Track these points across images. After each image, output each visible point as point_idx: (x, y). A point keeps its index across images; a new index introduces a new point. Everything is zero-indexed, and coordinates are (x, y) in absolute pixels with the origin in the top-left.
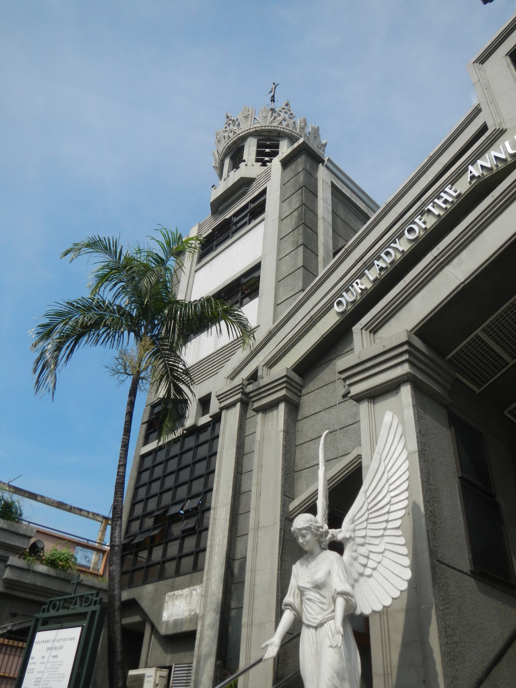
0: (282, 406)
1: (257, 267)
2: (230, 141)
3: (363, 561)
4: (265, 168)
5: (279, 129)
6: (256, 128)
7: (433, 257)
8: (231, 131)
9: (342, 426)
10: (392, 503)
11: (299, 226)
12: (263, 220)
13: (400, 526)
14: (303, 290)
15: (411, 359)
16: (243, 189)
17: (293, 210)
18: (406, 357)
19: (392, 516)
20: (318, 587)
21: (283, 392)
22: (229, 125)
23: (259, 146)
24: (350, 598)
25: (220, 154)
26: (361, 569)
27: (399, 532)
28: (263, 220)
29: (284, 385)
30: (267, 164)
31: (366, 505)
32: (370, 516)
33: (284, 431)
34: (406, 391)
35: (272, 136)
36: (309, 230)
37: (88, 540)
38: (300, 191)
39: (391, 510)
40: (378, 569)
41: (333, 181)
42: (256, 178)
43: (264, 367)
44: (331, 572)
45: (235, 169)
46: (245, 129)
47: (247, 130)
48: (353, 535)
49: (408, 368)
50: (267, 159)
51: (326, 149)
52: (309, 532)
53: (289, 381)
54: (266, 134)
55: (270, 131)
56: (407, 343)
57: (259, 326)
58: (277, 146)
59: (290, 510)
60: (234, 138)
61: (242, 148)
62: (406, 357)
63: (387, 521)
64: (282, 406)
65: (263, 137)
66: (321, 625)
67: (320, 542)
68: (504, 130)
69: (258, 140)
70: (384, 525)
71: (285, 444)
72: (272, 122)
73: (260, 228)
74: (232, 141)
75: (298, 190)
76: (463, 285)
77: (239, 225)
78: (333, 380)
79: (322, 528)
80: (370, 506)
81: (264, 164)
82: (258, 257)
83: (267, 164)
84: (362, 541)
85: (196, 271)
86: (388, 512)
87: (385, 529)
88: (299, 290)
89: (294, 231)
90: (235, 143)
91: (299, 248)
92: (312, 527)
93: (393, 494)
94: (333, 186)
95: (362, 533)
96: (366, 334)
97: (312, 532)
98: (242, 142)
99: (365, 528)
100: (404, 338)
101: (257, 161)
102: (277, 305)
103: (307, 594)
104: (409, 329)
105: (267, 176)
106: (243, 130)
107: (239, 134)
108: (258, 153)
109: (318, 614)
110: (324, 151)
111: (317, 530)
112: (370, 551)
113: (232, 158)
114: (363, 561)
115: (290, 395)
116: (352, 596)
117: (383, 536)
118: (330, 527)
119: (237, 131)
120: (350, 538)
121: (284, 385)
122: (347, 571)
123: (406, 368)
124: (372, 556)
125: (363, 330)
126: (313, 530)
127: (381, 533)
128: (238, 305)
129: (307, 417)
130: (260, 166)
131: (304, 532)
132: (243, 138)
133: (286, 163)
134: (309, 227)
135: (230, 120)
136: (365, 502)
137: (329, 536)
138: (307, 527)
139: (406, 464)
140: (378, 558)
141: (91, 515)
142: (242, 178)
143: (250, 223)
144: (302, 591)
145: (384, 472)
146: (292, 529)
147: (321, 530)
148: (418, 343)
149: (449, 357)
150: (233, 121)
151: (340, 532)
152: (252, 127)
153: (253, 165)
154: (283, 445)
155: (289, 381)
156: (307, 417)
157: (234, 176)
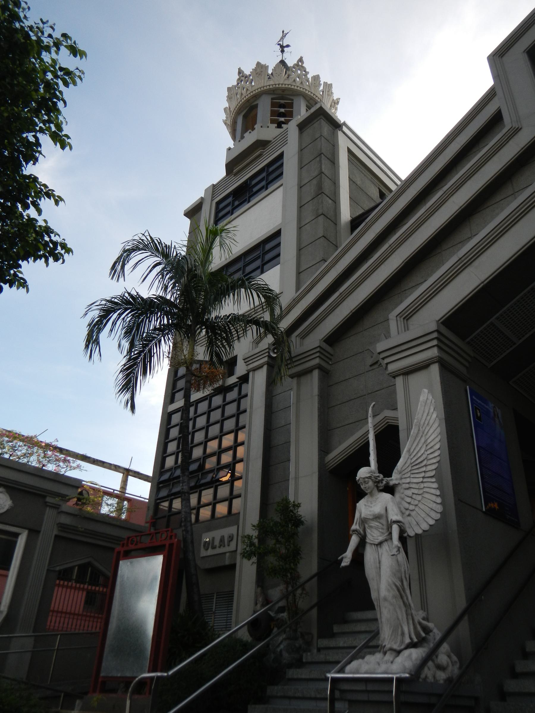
0: (316, 373)
1: (277, 234)
2: (243, 99)
3: (409, 500)
4: (280, 130)
5: (293, 87)
6: (269, 85)
7: (458, 259)
8: (244, 88)
9: (370, 392)
10: (428, 458)
11: (318, 195)
12: (282, 185)
13: (434, 475)
14: (325, 260)
15: (439, 344)
16: (260, 151)
17: (312, 178)
19: (429, 468)
20: (377, 517)
21: (317, 361)
22: (242, 81)
23: (273, 105)
24: (401, 524)
25: (233, 111)
26: (407, 506)
27: (434, 480)
28: (282, 185)
29: (318, 354)
30: (283, 125)
31: (409, 460)
32: (413, 468)
33: (318, 395)
34: (435, 369)
35: (285, 95)
36: (328, 199)
37: (114, 490)
38: (318, 159)
39: (427, 464)
40: (419, 505)
41: (349, 147)
42: (270, 141)
43: (297, 338)
44: (388, 508)
45: (250, 131)
46: (258, 87)
47: (260, 88)
48: (401, 482)
49: (437, 352)
50: (282, 119)
51: (339, 107)
52: (370, 480)
53: (322, 351)
55: (284, 90)
56: (437, 331)
57: (282, 292)
58: (291, 105)
59: (326, 462)
60: (247, 95)
61: (256, 106)
62: (435, 342)
63: (425, 472)
64: (316, 373)
65: (277, 96)
66: (380, 544)
67: (377, 487)
68: (520, 128)
69: (272, 99)
70: (422, 475)
71: (319, 407)
72: (285, 79)
73: (279, 193)
74: (245, 99)
75: (317, 157)
76: (482, 285)
77: (255, 190)
78: (362, 351)
79: (379, 477)
80: (413, 461)
81: (279, 125)
82: (277, 224)
83: (283, 125)
84: (407, 486)
86: (426, 466)
87: (423, 478)
88: (321, 260)
89: (314, 200)
90: (248, 101)
91: (320, 218)
92: (373, 476)
93: (429, 452)
94: (349, 151)
95: (408, 480)
96: (401, 320)
97: (372, 480)
98: (255, 101)
99: (409, 477)
100: (433, 327)
101: (272, 122)
102: (299, 273)
103: (370, 523)
104: (437, 319)
105: (283, 139)
106: (257, 88)
107: (252, 92)
108: (273, 113)
109: (378, 536)
110: (336, 109)
111: (376, 479)
112: (413, 493)
113: (245, 117)
114: (409, 500)
115: (324, 364)
116: (403, 523)
117: (422, 482)
118: (384, 477)
119: (250, 89)
120: (399, 484)
121: (318, 354)
122: (399, 505)
123: (434, 352)
124: (414, 496)
125: (398, 317)
126: (373, 478)
127: (421, 480)
128: (259, 271)
129: (337, 383)
130: (276, 127)
131: (366, 480)
132: (257, 96)
133: (302, 126)
134: (328, 196)
135: (243, 76)
136: (408, 458)
137: (384, 482)
138: (369, 476)
139: (438, 430)
140: (419, 498)
141: (113, 467)
143: (267, 189)
144: (364, 521)
145: (422, 436)
146: (357, 478)
147: (379, 478)
148: (444, 330)
150: (246, 77)
151: (391, 480)
152: (265, 85)
153: (268, 127)
154: (318, 408)
155: (322, 351)
156: (337, 383)
157: (250, 138)
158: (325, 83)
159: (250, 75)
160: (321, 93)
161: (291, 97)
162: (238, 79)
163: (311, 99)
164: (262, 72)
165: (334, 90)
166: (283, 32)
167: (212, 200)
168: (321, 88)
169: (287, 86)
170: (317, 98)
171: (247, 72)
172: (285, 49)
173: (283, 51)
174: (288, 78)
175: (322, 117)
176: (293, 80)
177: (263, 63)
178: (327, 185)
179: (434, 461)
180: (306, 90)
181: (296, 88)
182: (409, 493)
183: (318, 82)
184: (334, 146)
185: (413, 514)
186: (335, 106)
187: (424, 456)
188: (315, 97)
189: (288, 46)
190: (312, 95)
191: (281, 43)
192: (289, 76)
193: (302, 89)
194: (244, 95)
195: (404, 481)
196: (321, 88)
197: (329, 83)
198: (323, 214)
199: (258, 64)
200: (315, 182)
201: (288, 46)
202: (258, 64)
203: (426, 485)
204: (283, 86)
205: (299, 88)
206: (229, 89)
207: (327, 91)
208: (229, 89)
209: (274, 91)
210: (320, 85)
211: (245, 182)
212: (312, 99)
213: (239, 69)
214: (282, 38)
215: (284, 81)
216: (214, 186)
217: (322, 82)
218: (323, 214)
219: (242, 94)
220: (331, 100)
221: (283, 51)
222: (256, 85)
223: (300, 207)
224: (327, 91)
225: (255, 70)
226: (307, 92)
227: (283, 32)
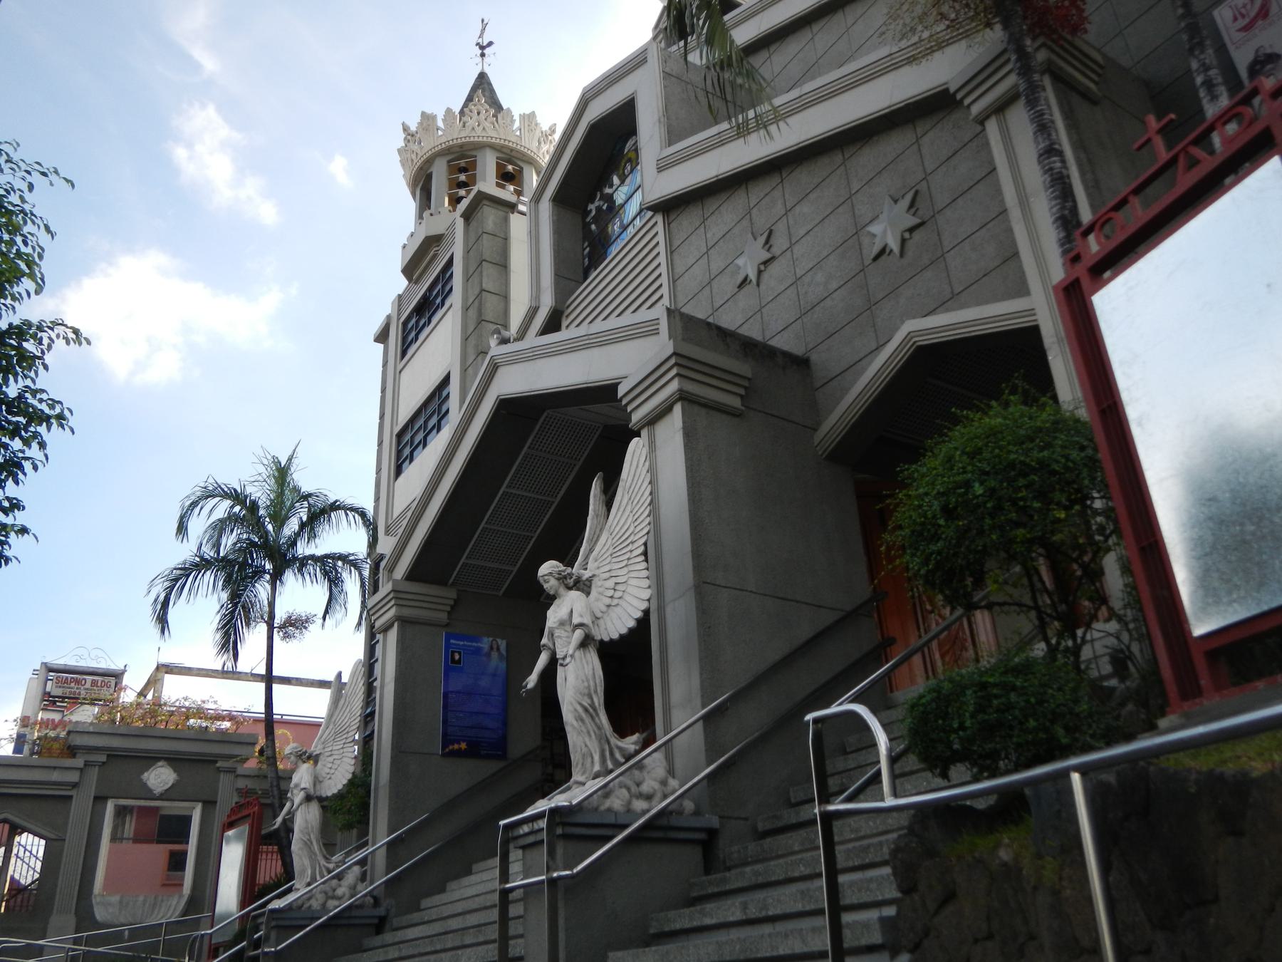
5: (472, 139)
18: (393, 602)
35: (466, 151)
42: (443, 235)
54: (458, 149)
55: (462, 146)
58: (473, 165)
65: (456, 155)
69: (449, 162)
72: (460, 130)
85: (400, 372)
90: (421, 168)
132: (429, 162)
135: (409, 135)
139: (362, 698)
140: (338, 762)
142: (426, 237)
149: (451, 581)
150: (413, 136)
158: (523, 117)
159: (417, 133)
160: (518, 133)
161: (474, 153)
162: (405, 139)
163: (502, 147)
164: (429, 125)
165: (539, 119)
166: (483, 21)
167: (398, 319)
168: (517, 124)
169: (463, 139)
170: (510, 144)
171: (413, 128)
172: (487, 51)
173: (483, 55)
174: (464, 126)
175: (485, 202)
176: (470, 128)
177: (429, 111)
178: (491, 303)
179: (355, 727)
180: (492, 138)
181: (476, 139)
182: (331, 759)
183: (509, 119)
184: (506, 239)
185: (333, 776)
186: (547, 139)
187: (347, 724)
188: (507, 143)
189: (490, 44)
190: (502, 142)
191: (480, 40)
192: (464, 123)
193: (485, 139)
194: (415, 161)
195: (326, 750)
196: (517, 124)
197: (527, 112)
198: (482, 352)
199: (423, 114)
200: (476, 302)
201: (490, 44)
202: (423, 114)
203: (345, 750)
204: (459, 141)
205: (481, 139)
206: (399, 150)
207: (526, 125)
208: (399, 150)
209: (448, 150)
210: (513, 121)
211: (425, 295)
212: (503, 146)
213: (403, 124)
214: (483, 30)
215: (459, 132)
216: (400, 296)
217: (516, 118)
218: (482, 352)
219: (412, 160)
220: (538, 134)
221: (483, 55)
222: (429, 145)
223: (466, 339)
224: (526, 125)
225: (421, 124)
226: (494, 140)
227: (483, 21)
